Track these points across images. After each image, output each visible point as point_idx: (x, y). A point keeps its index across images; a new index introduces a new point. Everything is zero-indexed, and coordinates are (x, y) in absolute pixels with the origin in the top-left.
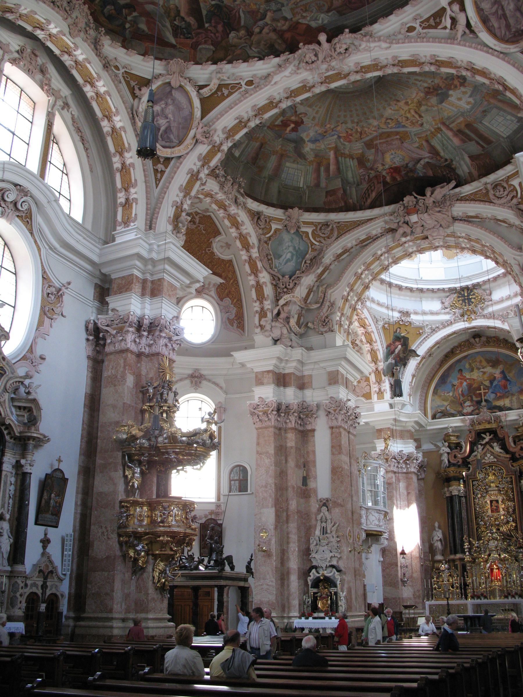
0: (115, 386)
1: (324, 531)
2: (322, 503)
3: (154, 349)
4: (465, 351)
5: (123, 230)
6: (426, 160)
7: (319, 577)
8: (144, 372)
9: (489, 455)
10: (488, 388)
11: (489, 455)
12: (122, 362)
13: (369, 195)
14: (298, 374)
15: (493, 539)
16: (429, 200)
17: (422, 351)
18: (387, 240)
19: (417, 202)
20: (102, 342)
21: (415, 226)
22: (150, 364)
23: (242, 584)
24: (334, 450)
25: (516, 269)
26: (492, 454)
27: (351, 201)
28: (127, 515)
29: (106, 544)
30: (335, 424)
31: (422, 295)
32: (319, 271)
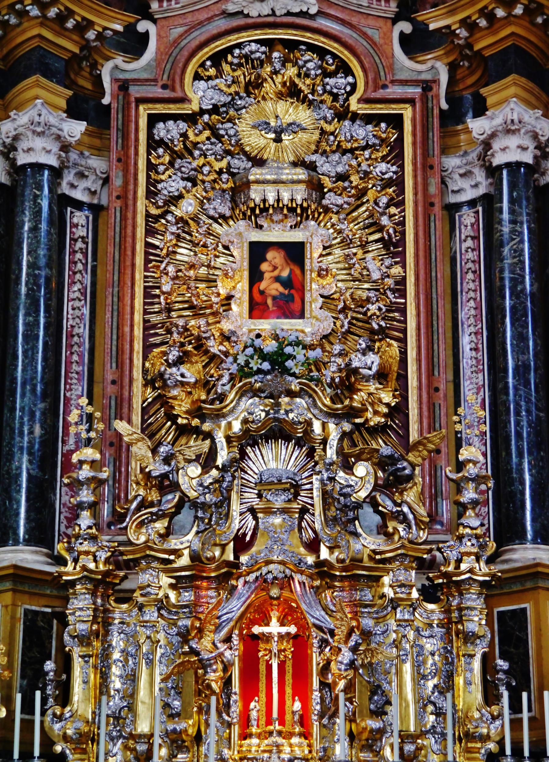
15: (278, 432)
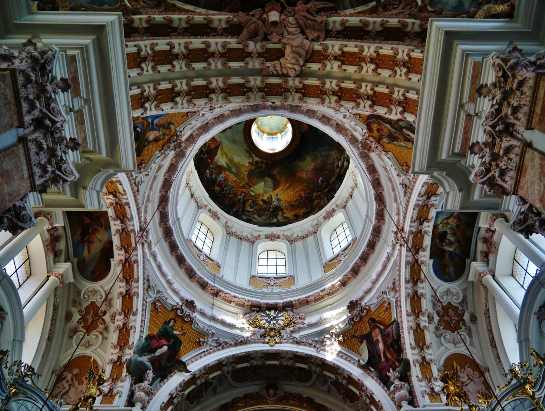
4: (252, 405)
17: (194, 367)
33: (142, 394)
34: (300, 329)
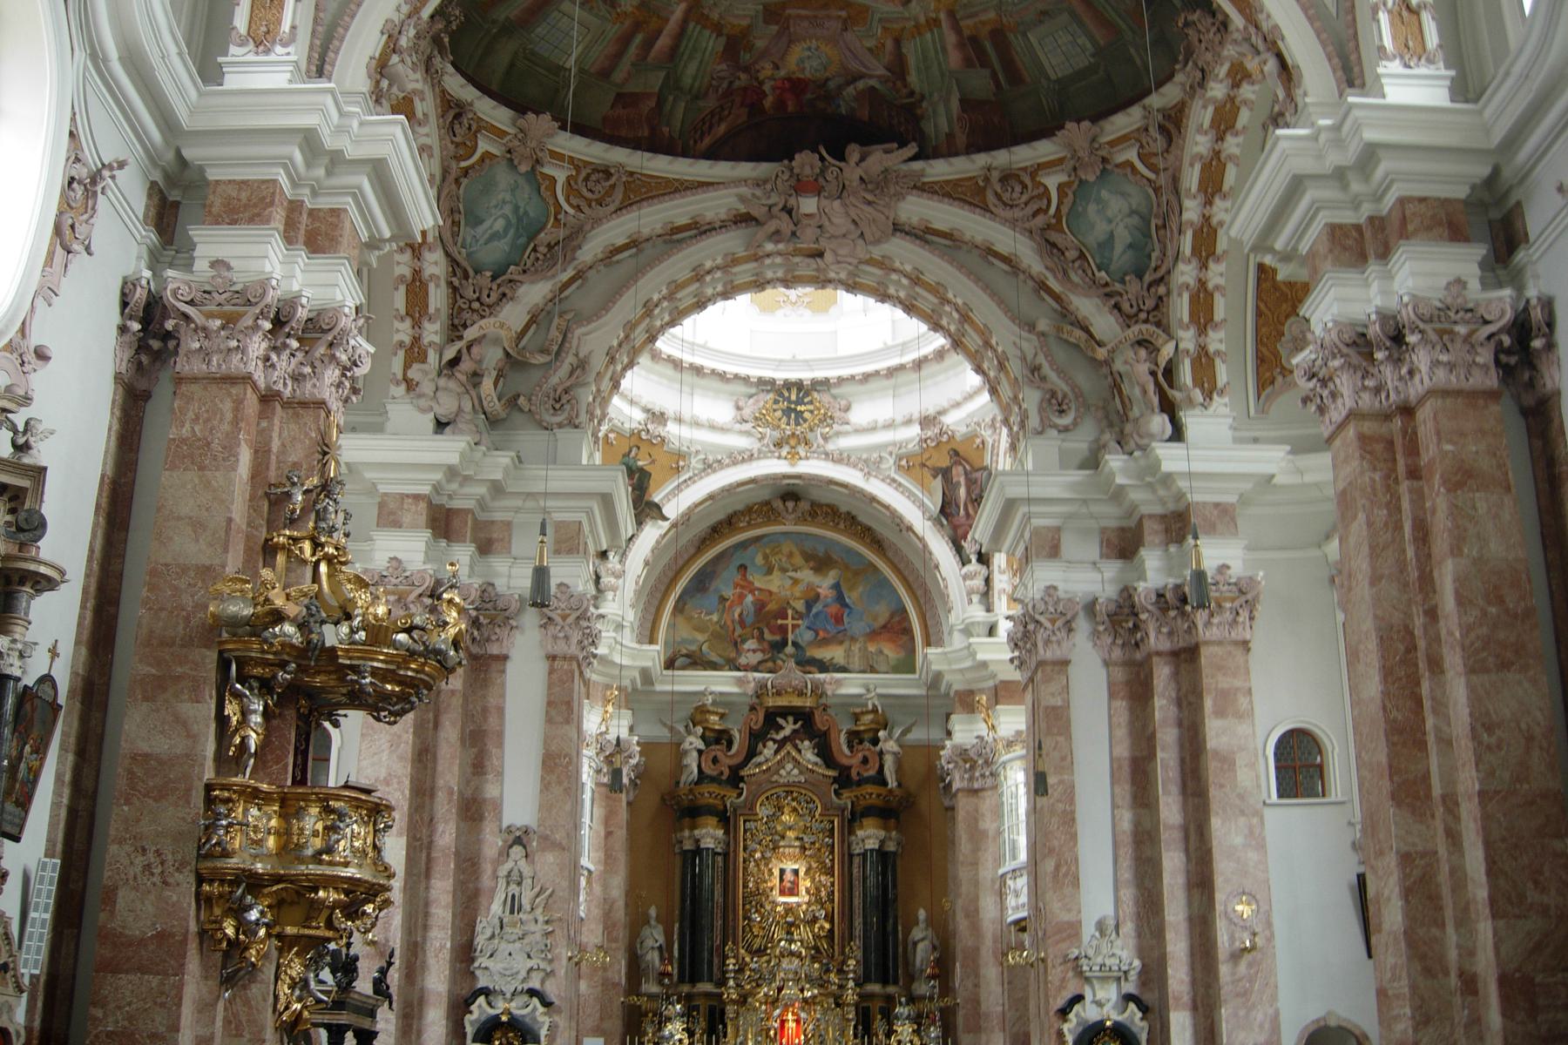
0: (202, 468)
1: (514, 905)
2: (511, 838)
3: (308, 390)
4: (759, 526)
5: (251, 57)
6: (872, 82)
7: (497, 1017)
8: (275, 445)
9: (789, 766)
10: (799, 615)
11: (789, 766)
12: (227, 407)
13: (711, 127)
14: (482, 516)
16: (852, 172)
18: (731, 242)
19: (823, 171)
20: (155, 344)
21: (805, 221)
22: (292, 426)
23: (365, 1023)
24: (553, 713)
25: (1015, 367)
26: (797, 763)
27: (666, 130)
28: (230, 825)
29: (150, 899)
30: (560, 648)
31: (696, 380)
32: (565, 277)
33: (613, 580)
34: (838, 434)
